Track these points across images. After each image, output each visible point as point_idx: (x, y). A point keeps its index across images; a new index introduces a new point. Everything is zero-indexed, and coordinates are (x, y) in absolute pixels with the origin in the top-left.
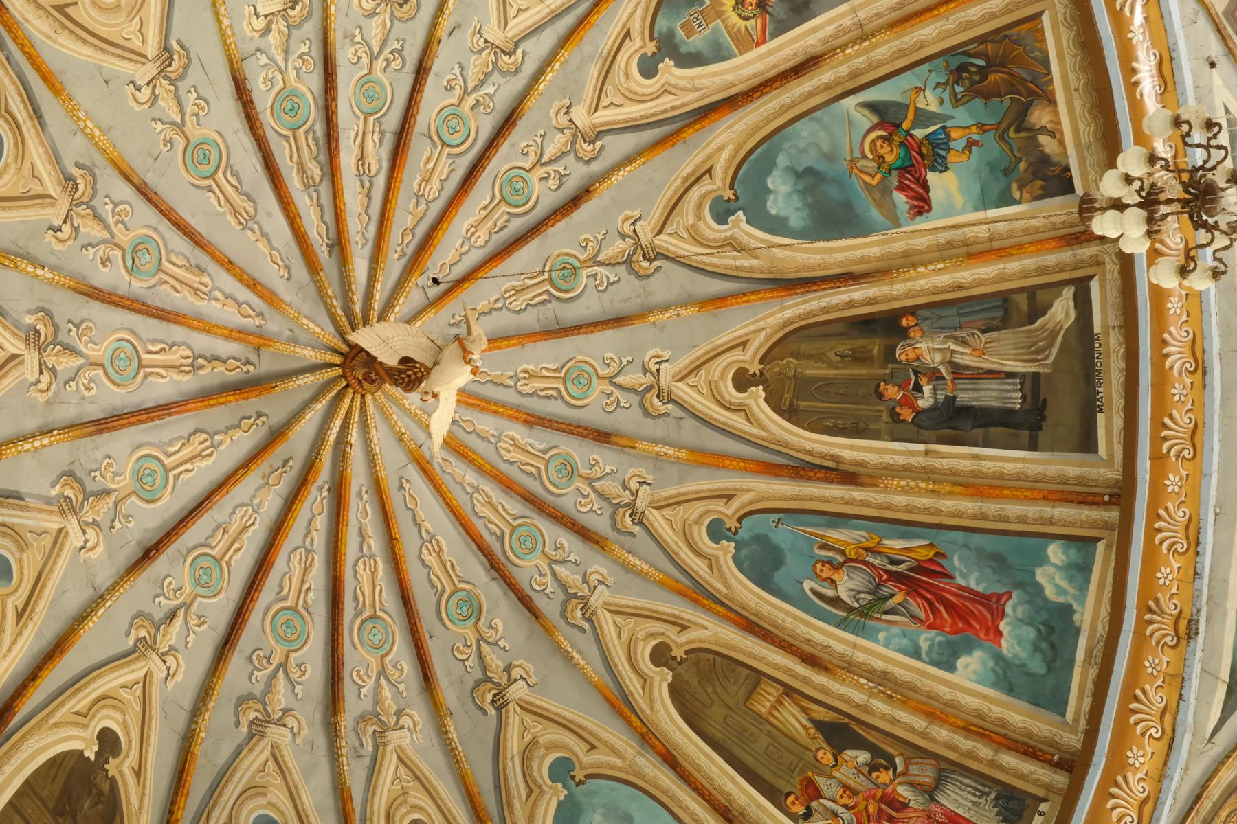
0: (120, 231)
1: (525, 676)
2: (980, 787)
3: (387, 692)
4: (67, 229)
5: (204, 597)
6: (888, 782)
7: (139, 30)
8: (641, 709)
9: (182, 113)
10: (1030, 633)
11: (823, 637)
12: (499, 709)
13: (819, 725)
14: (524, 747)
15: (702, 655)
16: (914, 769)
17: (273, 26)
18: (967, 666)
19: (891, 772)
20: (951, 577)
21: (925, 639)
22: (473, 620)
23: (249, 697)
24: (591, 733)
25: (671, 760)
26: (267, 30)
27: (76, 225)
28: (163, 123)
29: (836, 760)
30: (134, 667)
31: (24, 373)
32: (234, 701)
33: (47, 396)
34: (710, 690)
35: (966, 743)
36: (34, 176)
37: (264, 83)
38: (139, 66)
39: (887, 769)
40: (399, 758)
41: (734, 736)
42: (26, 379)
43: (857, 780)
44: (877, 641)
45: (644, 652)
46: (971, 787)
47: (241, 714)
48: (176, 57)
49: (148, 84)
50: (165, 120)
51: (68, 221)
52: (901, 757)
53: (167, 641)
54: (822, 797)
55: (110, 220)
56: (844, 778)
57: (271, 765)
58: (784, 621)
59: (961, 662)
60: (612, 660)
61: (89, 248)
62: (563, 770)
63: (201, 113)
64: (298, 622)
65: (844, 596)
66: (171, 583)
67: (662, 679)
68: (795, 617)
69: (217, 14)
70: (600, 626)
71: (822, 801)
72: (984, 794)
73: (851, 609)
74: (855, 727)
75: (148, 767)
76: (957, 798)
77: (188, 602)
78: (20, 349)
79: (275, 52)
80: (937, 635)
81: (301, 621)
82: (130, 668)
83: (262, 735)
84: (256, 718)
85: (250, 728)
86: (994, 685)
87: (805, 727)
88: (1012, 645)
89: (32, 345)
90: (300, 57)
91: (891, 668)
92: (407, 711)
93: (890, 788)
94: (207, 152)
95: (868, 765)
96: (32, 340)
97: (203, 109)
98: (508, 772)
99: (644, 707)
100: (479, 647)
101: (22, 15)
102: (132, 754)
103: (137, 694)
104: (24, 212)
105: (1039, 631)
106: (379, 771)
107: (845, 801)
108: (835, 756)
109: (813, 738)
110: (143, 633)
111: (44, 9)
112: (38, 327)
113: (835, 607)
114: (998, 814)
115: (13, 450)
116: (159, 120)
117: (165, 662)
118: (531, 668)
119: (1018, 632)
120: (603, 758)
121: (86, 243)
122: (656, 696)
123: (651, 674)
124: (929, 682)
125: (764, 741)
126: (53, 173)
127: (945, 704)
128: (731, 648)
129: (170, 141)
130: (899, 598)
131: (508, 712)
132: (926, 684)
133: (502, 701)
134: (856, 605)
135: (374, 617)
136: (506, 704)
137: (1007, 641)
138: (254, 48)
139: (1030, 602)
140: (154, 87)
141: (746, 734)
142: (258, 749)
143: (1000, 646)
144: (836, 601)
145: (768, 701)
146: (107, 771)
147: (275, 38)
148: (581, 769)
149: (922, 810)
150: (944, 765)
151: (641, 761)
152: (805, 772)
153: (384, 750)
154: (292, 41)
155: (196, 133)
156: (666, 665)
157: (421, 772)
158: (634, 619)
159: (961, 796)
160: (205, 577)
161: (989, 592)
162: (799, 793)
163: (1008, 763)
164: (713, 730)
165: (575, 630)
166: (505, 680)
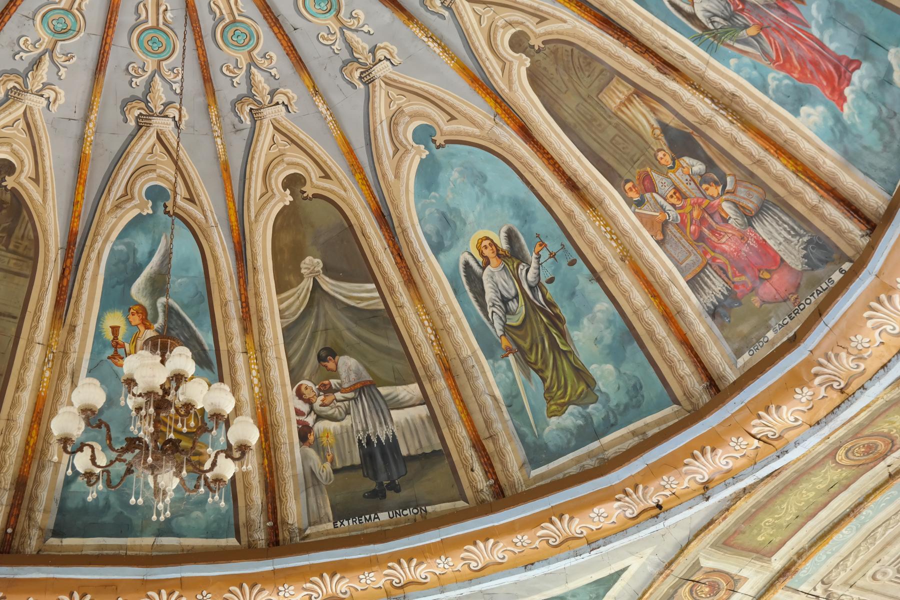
1: (388, 57)
2: (796, 228)
3: (258, 76)
5: (64, 40)
6: (715, 196)
8: (500, 88)
10: (872, 110)
11: (679, 47)
12: (366, 84)
13: (665, 128)
14: (391, 115)
15: (559, 45)
16: (742, 192)
18: (809, 115)
19: (720, 188)
20: (808, 26)
21: (775, 77)
22: (333, 13)
23: (134, 99)
24: (451, 106)
25: (526, 132)
29: (674, 164)
30: (11, 110)
32: (119, 104)
34: (566, 78)
35: (796, 183)
39: (717, 184)
40: (275, 128)
41: (583, 122)
43: (688, 186)
44: (728, 66)
45: (504, 38)
46: (788, 225)
47: (127, 113)
52: (733, 178)
53: (39, 82)
54: (655, 192)
56: (677, 181)
57: (159, 147)
58: (642, 24)
59: (804, 110)
60: (473, 44)
62: (425, 135)
64: (163, 38)
65: (700, 15)
66: (27, 40)
67: (521, 64)
68: (653, 24)
70: (460, 14)
71: (654, 194)
72: (797, 234)
73: (705, 29)
74: (697, 138)
75: (48, 170)
76: (772, 230)
77: (50, 47)
80: (785, 77)
81: (165, 36)
82: (7, 112)
83: (149, 126)
84: (141, 114)
85: (137, 122)
86: (831, 143)
87: (652, 126)
88: (853, 113)
91: (739, 93)
92: (281, 90)
93: (716, 202)
95: (701, 176)
98: (377, 133)
99: (503, 86)
100: (343, 34)
102: (26, 169)
103: (20, 127)
105: (880, 111)
106: (257, 140)
107: (674, 201)
108: (673, 160)
109: (657, 139)
110: (10, 85)
113: (692, 24)
114: (804, 257)
117: (42, 96)
118: (395, 49)
119: (861, 103)
120: (462, 127)
122: (515, 77)
123: (510, 58)
124: (773, 116)
125: (611, 132)
127: (785, 141)
128: (589, 42)
130: (752, 31)
131: (374, 87)
132: (770, 118)
133: (368, 77)
134: (710, 26)
135: (234, 21)
136: (372, 80)
137: (849, 108)
139: (875, 78)
141: (594, 123)
142: (145, 137)
143: (842, 110)
144: (692, 17)
145: (619, 98)
146: (6, 186)
148: (441, 135)
149: (738, 230)
150: (769, 197)
151: (498, 131)
152: (644, 166)
153: (261, 123)
156: (524, 52)
157: (298, 137)
158: (494, 7)
159: (777, 230)
160: (60, 26)
161: (840, 53)
162: (636, 183)
163: (830, 215)
164: (566, 114)
165: (435, 17)
166: (370, 61)
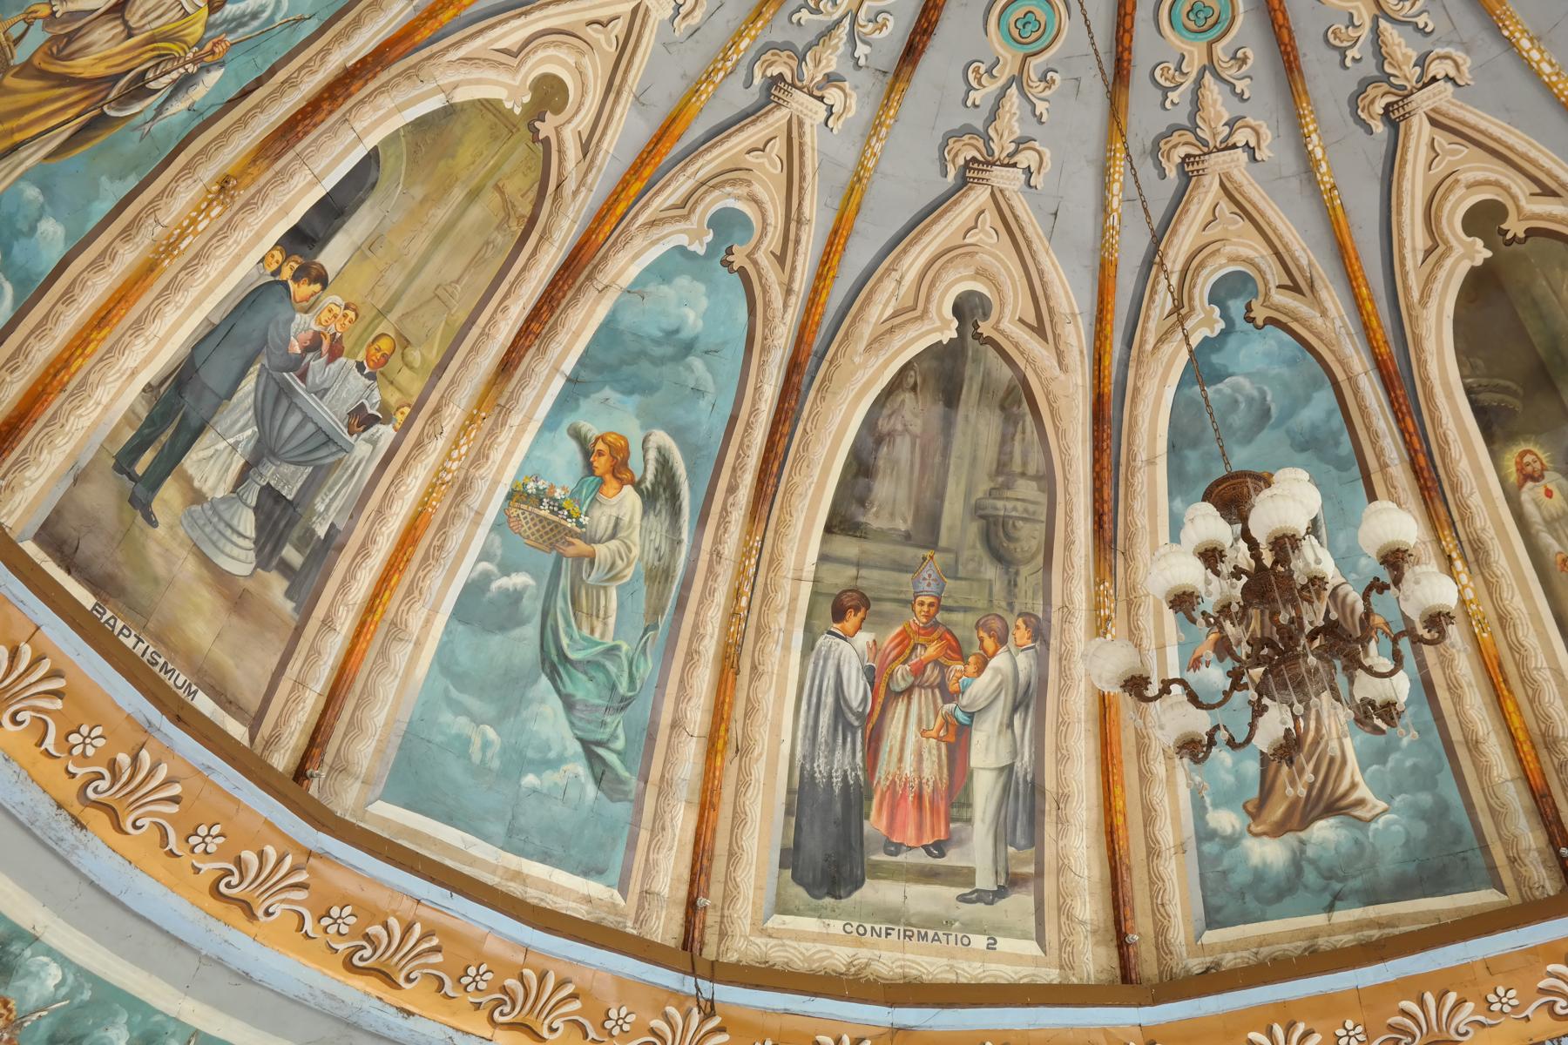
0: (1191, 64)
4: (1241, 137)
7: (976, 227)
9: (1002, 94)
17: (819, 77)
26: (831, 79)
27: (1227, 130)
28: (1034, 106)
31: (1448, 101)
33: (1459, 55)
36: (1215, 219)
37: (885, 25)
38: (1007, 193)
42: (1454, 95)
48: (961, 161)
49: (1014, 165)
50: (1029, 108)
51: (1231, 142)
55: (1188, 83)
61: (1238, 90)
63: (983, 69)
69: (878, 162)
78: (1421, 120)
79: (841, 44)
89: (1407, 109)
90: (817, 11)
94: (1019, 25)
96: (1402, 112)
97: (977, 70)
101: (1082, 362)
104: (1262, 204)
111: (1057, 348)
112: (1382, 112)
115: (1561, 86)
116: (1035, 115)
121: (1236, 99)
126: (1195, 200)
129: (1043, 78)
138: (861, 73)
140: (1010, 155)
147: (829, 61)
154: (810, 38)
155: (1010, 60)
